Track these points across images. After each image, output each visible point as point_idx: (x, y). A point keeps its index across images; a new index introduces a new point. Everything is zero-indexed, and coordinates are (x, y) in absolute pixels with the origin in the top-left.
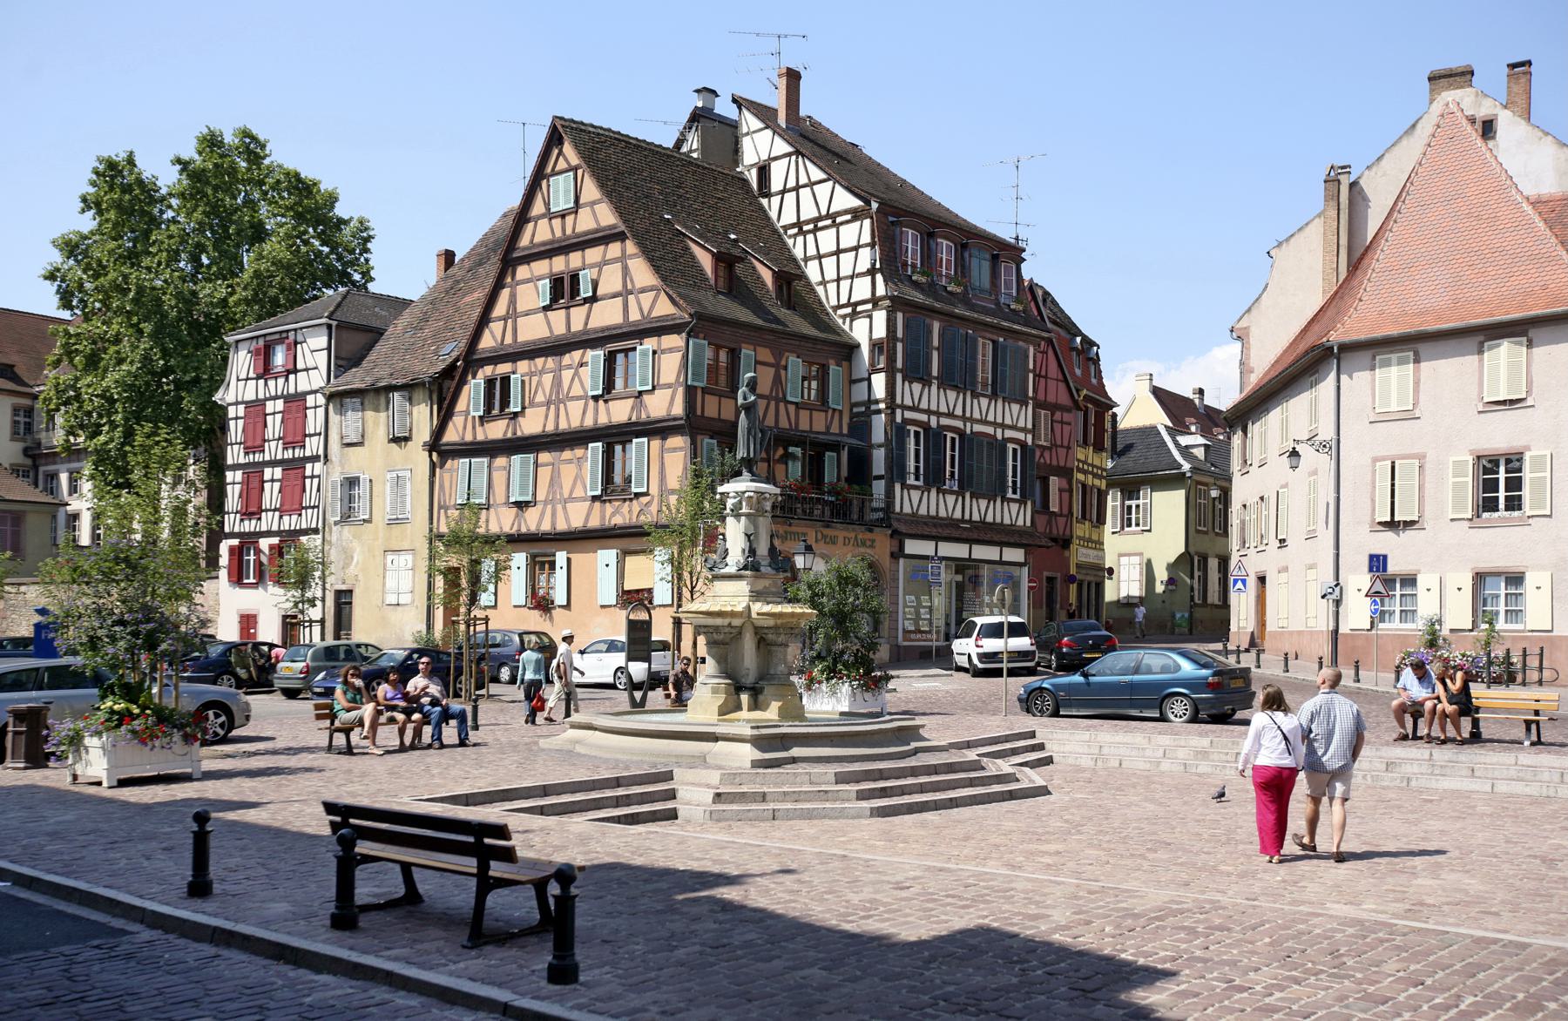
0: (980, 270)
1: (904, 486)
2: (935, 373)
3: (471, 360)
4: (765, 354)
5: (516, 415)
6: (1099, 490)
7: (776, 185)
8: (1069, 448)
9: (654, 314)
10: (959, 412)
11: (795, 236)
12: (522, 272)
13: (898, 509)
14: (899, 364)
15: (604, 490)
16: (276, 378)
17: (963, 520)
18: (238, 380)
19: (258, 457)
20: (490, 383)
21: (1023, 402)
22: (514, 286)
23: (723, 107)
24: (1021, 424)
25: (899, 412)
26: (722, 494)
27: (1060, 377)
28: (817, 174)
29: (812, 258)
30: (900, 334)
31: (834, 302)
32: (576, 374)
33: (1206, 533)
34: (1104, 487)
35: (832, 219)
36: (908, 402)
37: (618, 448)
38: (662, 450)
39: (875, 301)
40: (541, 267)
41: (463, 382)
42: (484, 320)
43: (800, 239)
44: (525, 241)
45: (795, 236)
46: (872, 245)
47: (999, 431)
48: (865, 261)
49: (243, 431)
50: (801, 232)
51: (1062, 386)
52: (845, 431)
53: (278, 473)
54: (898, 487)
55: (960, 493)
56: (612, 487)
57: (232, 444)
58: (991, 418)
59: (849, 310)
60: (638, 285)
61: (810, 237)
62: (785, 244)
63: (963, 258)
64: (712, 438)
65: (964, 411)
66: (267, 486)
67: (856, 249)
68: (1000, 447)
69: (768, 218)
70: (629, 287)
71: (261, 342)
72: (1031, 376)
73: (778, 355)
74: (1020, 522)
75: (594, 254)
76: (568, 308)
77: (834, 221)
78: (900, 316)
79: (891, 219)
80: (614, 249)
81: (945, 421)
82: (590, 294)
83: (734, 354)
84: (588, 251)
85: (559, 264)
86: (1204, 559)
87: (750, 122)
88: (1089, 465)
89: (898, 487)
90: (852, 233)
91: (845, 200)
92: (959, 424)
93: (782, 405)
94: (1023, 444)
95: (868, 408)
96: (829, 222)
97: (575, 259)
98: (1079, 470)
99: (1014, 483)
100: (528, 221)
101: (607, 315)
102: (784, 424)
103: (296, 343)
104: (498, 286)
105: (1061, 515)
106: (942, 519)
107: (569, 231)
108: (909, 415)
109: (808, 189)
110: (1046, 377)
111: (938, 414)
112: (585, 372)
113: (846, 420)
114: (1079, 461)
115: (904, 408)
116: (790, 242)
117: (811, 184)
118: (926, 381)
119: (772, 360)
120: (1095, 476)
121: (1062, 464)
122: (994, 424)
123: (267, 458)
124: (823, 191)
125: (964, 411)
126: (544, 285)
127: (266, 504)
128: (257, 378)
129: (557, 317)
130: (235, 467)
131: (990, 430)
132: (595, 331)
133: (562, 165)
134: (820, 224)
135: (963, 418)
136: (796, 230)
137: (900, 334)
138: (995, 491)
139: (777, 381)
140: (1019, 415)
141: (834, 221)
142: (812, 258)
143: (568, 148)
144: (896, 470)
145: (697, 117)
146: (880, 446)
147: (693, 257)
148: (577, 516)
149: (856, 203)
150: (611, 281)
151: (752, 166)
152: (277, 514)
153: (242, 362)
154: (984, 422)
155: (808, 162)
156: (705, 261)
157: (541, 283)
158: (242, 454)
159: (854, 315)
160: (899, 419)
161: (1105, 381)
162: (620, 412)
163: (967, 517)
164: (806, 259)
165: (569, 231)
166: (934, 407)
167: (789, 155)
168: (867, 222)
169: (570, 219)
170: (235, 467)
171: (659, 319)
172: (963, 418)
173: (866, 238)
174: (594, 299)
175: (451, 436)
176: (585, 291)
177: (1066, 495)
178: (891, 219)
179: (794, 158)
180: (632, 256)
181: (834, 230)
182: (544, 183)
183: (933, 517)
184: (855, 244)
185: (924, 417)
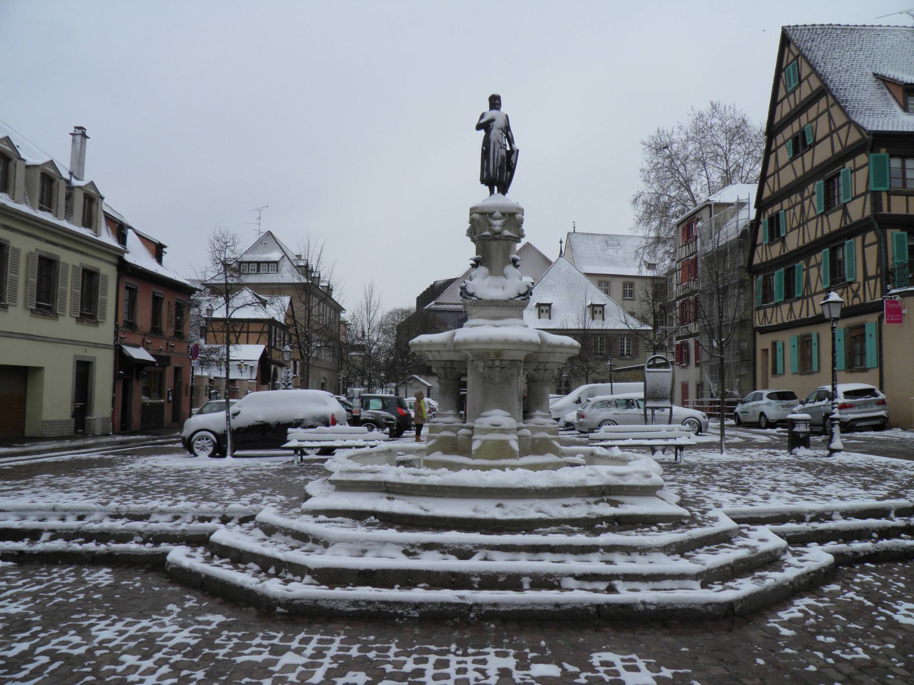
5: (784, 237)
12: (780, 139)
15: (832, 283)
20: (771, 219)
22: (776, 151)
32: (811, 201)
38: (864, 246)
40: (788, 133)
56: (837, 279)
60: (838, 124)
64: (902, 230)
75: (812, 112)
76: (802, 155)
85: (795, 127)
97: (803, 118)
100: (778, 104)
101: (822, 153)
112: (815, 198)
128: (685, 245)
129: (798, 163)
132: (817, 167)
133: (791, 58)
162: (835, 221)
169: (797, 92)
174: (815, 143)
175: (756, 261)
176: (810, 142)
182: (783, 74)
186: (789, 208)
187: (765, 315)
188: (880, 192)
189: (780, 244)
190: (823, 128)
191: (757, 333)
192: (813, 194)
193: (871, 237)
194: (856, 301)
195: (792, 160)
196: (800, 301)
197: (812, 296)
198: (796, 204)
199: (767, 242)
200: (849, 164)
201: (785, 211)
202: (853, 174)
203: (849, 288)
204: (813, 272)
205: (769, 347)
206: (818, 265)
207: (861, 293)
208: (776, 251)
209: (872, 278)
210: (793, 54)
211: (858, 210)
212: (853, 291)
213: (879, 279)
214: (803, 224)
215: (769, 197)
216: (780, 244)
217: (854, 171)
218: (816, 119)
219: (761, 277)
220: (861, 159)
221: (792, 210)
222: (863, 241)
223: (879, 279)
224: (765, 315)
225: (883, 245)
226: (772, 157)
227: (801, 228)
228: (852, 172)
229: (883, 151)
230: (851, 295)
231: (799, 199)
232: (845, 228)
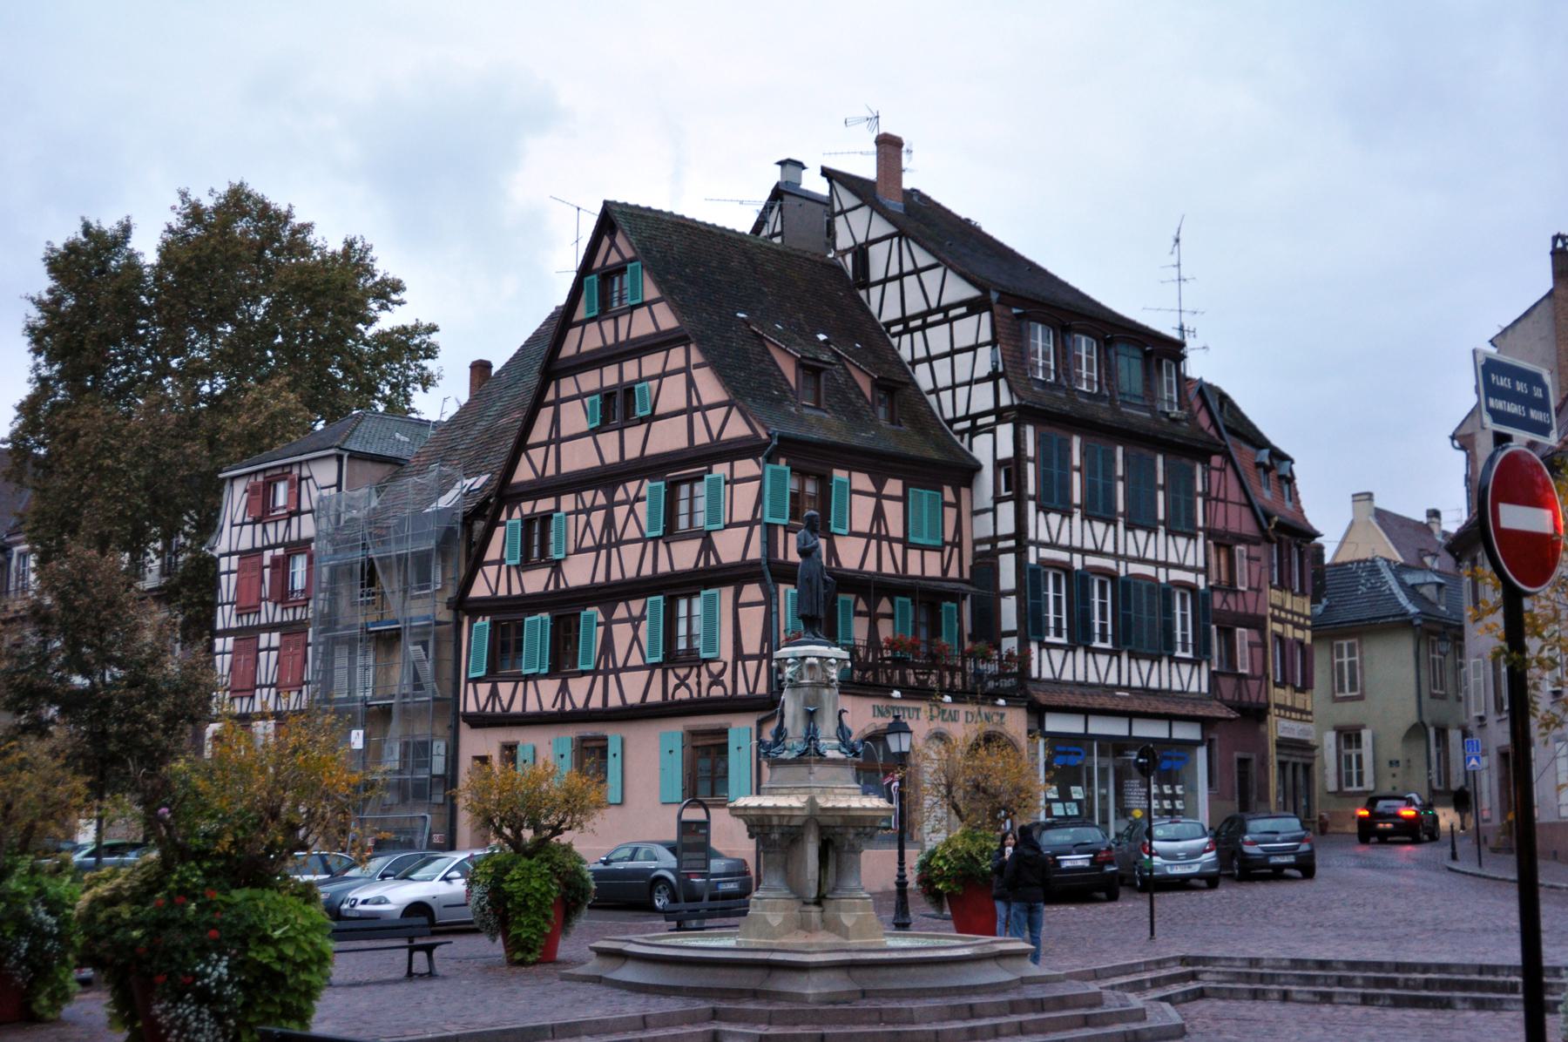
0: (1129, 370)
1: (1043, 645)
2: (1077, 499)
3: (504, 494)
4: (862, 481)
5: (559, 562)
6: (1301, 643)
7: (876, 273)
8: (1259, 590)
9: (725, 436)
10: (1109, 548)
11: (899, 334)
12: (567, 386)
13: (1035, 674)
14: (1031, 490)
16: (276, 522)
17: (1119, 687)
18: (233, 525)
19: (252, 620)
20: (528, 522)
21: (1191, 536)
22: (558, 402)
23: (814, 183)
24: (1190, 562)
25: (1032, 549)
26: (778, 660)
27: (1244, 501)
28: (923, 259)
29: (921, 361)
30: (1030, 451)
31: (949, 414)
32: (632, 511)
33: (1443, 698)
34: (1308, 640)
35: (945, 314)
36: (1043, 536)
37: (683, 604)
38: (737, 605)
39: (1000, 414)
40: (589, 380)
41: (494, 523)
42: (521, 446)
43: (906, 338)
44: (568, 350)
45: (899, 334)
46: (993, 343)
47: (1162, 571)
48: (984, 368)
49: (236, 588)
50: (908, 331)
51: (1246, 512)
52: (967, 575)
53: (276, 639)
54: (1034, 647)
55: (1114, 653)
57: (223, 604)
58: (1150, 555)
59: (967, 424)
60: (706, 401)
61: (918, 336)
62: (890, 344)
63: (1107, 358)
65: (1116, 547)
66: (263, 655)
67: (973, 348)
68: (1168, 590)
69: (869, 313)
70: (695, 403)
71: (260, 479)
72: (1200, 501)
73: (879, 484)
74: (1194, 688)
75: (653, 364)
76: (621, 430)
77: (946, 315)
78: (1030, 432)
79: (1015, 311)
80: (677, 357)
81: (1092, 561)
82: (648, 412)
83: (824, 480)
84: (645, 360)
85: (610, 376)
86: (1442, 733)
87: (847, 199)
88: (1287, 612)
89: (1034, 647)
90: (971, 329)
91: (958, 290)
92: (1109, 563)
93: (885, 544)
94: (1192, 588)
95: (994, 546)
96: (940, 316)
97: (630, 370)
98: (1276, 619)
99: (1184, 637)
101: (668, 437)
102: (888, 568)
103: (301, 479)
104: (538, 403)
105: (1253, 677)
106: (1092, 685)
107: (622, 337)
108: (1046, 553)
109: (914, 277)
110: (1225, 501)
111: (1084, 552)
112: (641, 508)
113: (968, 562)
114: (1274, 606)
115: (1039, 544)
116: (895, 341)
117: (917, 271)
118: (1066, 513)
119: (872, 489)
120: (1297, 626)
121: (1251, 610)
122: (1156, 563)
123: (263, 621)
124: (932, 279)
125: (1116, 547)
126: (593, 403)
127: (262, 678)
128: (254, 523)
129: (609, 441)
130: (226, 633)
131: (1149, 570)
134: (930, 319)
135: (1115, 556)
136: (900, 327)
137: (1030, 452)
138: (1160, 649)
139: (879, 515)
140: (1191, 552)
141: (946, 315)
142: (921, 361)
143: (620, 240)
144: (1032, 625)
145: (778, 194)
146: (1009, 593)
147: (775, 364)
148: (634, 688)
149: (970, 292)
150: (673, 394)
151: (846, 251)
152: (273, 690)
153: (236, 501)
154: (1142, 560)
155: (913, 245)
156: (789, 369)
157: (586, 400)
158: (234, 618)
159: (974, 431)
160: (1032, 560)
161: (1304, 505)
162: (685, 556)
163: (1124, 682)
164: (914, 362)
165: (622, 337)
166: (1077, 543)
167: (889, 237)
168: (986, 317)
169: (623, 322)
170: (226, 633)
171: (731, 441)
172: (1115, 556)
173: (986, 335)
174: (653, 418)
175: (479, 590)
177: (1258, 652)
178: (1015, 311)
179: (896, 240)
180: (697, 366)
181: (946, 326)
183: (1080, 684)
184: (971, 342)
185: (1064, 556)
186: (577, 512)
187: (494, 693)
188: (776, 525)
189: (548, 570)
190: (673, 394)
191: (464, 727)
192: (638, 499)
193: (752, 592)
194: (717, 691)
195: (593, 432)
196: (588, 679)
197: (617, 671)
198: (594, 508)
199: (518, 561)
200: (721, 470)
201: (568, 514)
202: (728, 486)
203: (703, 670)
204: (622, 634)
205: (495, 753)
206: (635, 622)
207: (727, 678)
208: (535, 581)
209: (751, 657)
210: (619, 251)
211: (730, 547)
212: (710, 674)
213: (765, 661)
214: (610, 542)
215: (530, 482)
216: (548, 570)
217: (732, 481)
218: (661, 377)
219: (484, 622)
220: (746, 467)
221: (582, 518)
222: (737, 595)
223: (765, 661)
224: (494, 693)
225: (774, 609)
226: (545, 415)
227: (603, 553)
228: (726, 483)
229: (783, 461)
230: (705, 679)
231: (601, 499)
232: (703, 571)
